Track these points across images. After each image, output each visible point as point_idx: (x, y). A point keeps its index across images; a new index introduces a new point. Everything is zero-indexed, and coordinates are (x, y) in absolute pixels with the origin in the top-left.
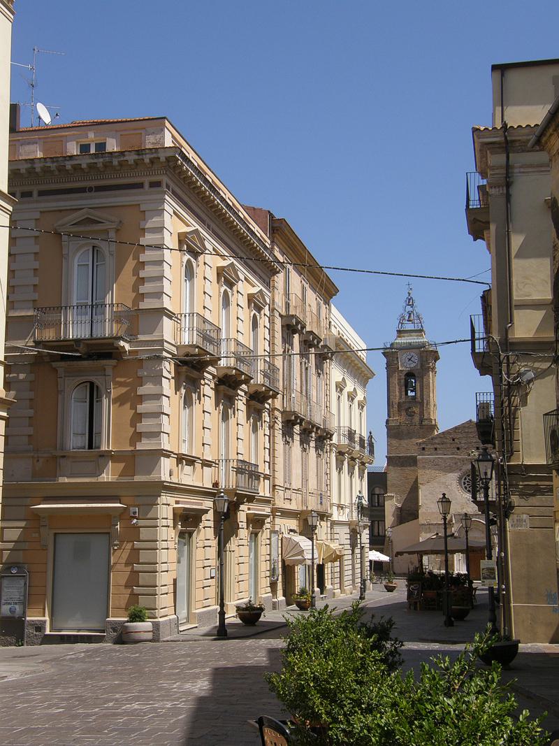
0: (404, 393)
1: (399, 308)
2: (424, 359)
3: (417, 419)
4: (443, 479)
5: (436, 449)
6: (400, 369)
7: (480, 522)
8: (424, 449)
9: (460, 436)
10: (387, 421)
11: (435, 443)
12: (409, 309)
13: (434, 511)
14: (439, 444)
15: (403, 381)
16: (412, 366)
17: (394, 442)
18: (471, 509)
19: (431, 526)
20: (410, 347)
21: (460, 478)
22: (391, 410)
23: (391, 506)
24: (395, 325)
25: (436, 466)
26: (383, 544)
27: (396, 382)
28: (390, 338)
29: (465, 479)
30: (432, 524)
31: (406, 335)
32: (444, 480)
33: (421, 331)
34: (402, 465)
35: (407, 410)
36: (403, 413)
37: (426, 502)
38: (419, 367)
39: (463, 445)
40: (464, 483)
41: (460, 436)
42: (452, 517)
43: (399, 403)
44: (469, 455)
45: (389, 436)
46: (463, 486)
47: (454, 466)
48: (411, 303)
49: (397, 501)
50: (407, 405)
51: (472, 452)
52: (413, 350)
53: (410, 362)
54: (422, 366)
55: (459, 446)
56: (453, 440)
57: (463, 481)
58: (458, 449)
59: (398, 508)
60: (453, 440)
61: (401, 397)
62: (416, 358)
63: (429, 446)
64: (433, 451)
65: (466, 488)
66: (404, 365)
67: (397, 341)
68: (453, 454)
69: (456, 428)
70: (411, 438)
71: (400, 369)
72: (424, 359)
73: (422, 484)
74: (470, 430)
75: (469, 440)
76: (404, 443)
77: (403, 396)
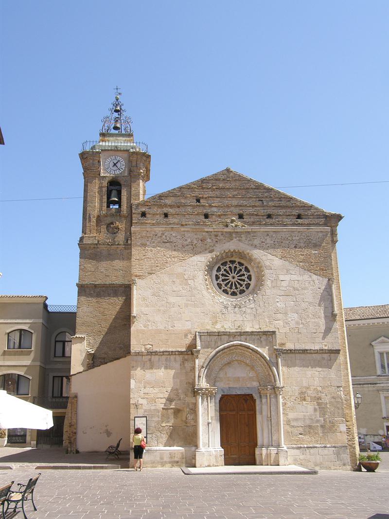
0: (105, 205)
1: (105, 110)
2: (134, 164)
3: (121, 237)
4: (178, 268)
5: (166, 215)
6: (102, 175)
7: (248, 348)
8: (144, 214)
9: (211, 194)
10: (81, 239)
11: (166, 205)
12: (116, 115)
13: (161, 327)
14: (171, 206)
15: (105, 190)
16: (118, 172)
17: (90, 265)
18: (230, 325)
19: (155, 358)
20: (116, 150)
21: (210, 268)
22: (88, 224)
23: (79, 352)
24: (98, 127)
25: (166, 242)
26: (65, 407)
27: (96, 189)
28: (91, 138)
29: (219, 270)
30: (156, 353)
31: (111, 139)
32: (180, 270)
33: (130, 135)
34: (98, 295)
35: (108, 225)
36: (103, 228)
37: (145, 310)
38: (126, 174)
39: (215, 209)
40: (217, 278)
41: (211, 194)
42: (195, 339)
43: (98, 216)
44: (227, 226)
45: (82, 256)
46: (216, 283)
47: (199, 244)
48: (118, 108)
49: (89, 344)
50: (109, 220)
51: (232, 221)
52: (120, 154)
53: (115, 168)
54: (130, 171)
55: (208, 211)
56: (198, 201)
57: (215, 273)
58: (206, 216)
59: (89, 355)
60: (198, 201)
61: (101, 209)
62: (122, 165)
63: (151, 211)
64: (161, 218)
65: (219, 285)
66: (107, 171)
67: (101, 144)
68: (198, 224)
69: (203, 181)
70: (112, 260)
71: (102, 175)
72: (134, 164)
73: (139, 276)
74: (228, 186)
75: (226, 202)
76: (104, 265)
77: (105, 208)
